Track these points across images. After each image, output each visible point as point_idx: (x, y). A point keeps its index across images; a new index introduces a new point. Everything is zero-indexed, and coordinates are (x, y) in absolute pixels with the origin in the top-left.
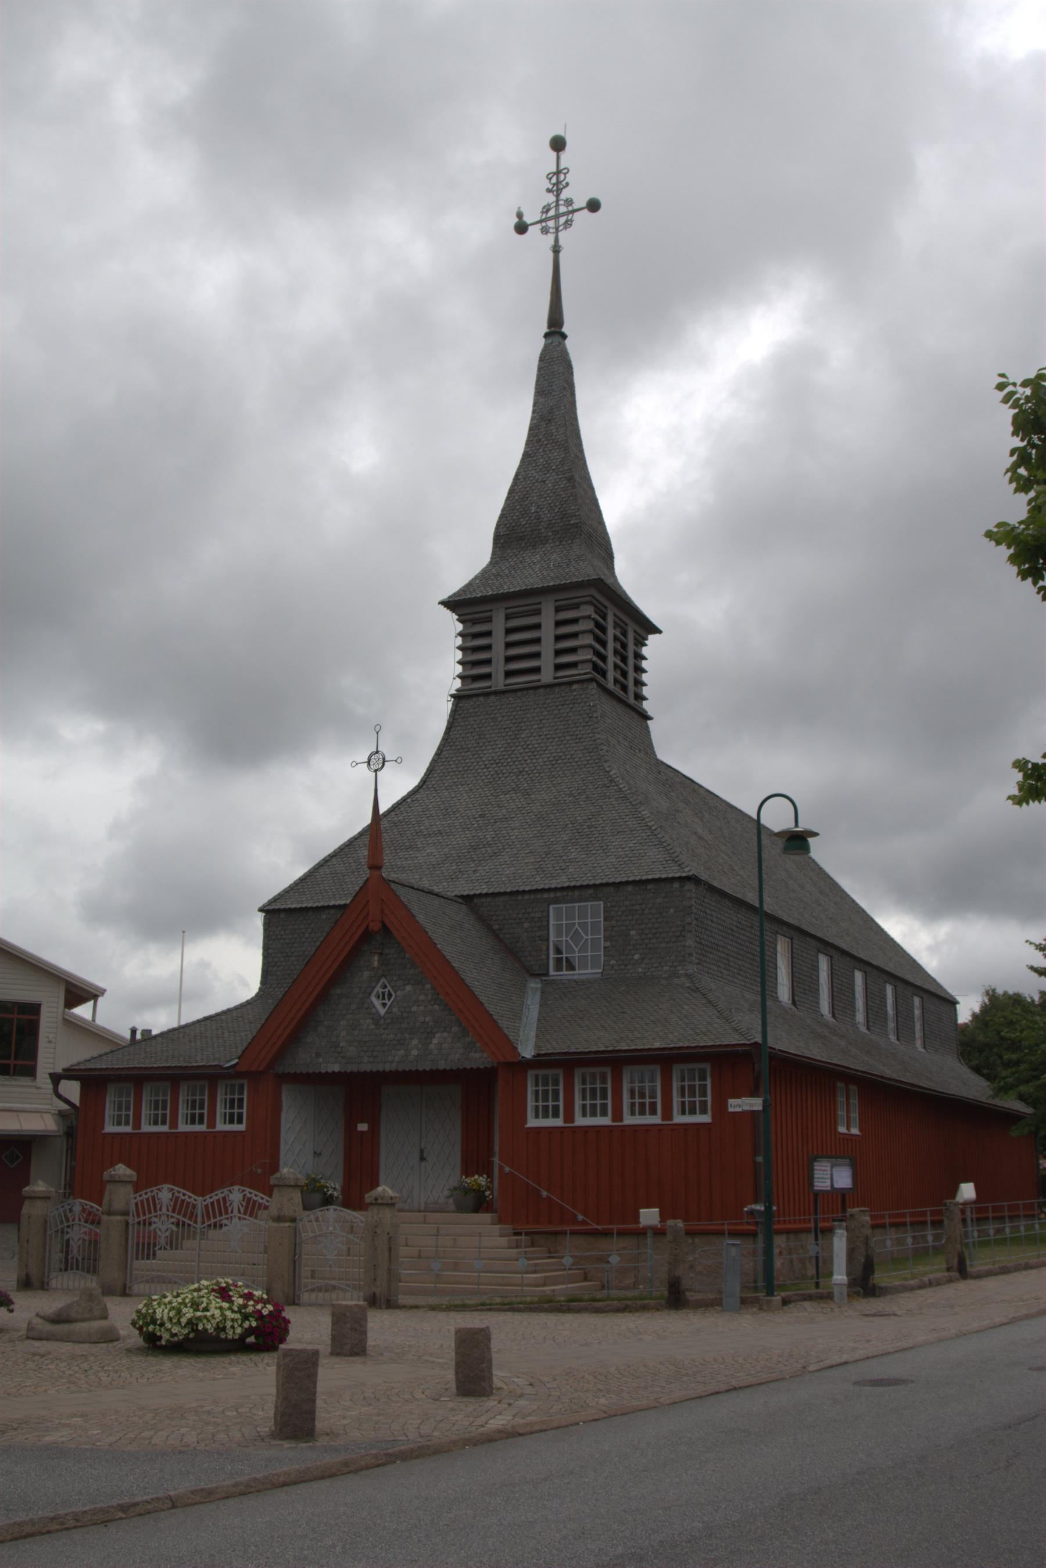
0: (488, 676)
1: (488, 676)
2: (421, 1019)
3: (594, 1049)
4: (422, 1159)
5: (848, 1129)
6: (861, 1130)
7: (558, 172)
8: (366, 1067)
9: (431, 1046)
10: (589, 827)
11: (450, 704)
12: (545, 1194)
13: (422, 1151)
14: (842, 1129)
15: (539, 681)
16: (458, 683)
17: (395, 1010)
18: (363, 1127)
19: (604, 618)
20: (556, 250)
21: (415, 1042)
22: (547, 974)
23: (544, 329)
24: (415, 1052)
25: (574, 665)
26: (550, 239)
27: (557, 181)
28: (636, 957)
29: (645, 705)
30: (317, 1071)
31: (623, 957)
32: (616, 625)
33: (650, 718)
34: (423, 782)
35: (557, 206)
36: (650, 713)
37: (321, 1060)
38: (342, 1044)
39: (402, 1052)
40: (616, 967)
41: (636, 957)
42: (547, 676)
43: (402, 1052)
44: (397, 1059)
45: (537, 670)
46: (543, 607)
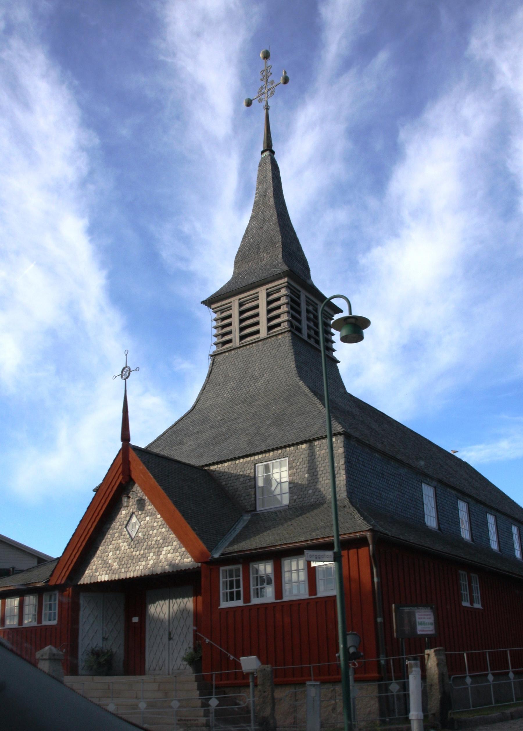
0: (230, 341)
1: (230, 341)
2: (155, 539)
3: (259, 546)
4: (170, 639)
5: (472, 603)
6: (482, 606)
8: (123, 576)
9: (161, 557)
10: (282, 415)
11: (210, 361)
12: (232, 657)
13: (170, 634)
14: (466, 604)
15: (259, 338)
16: (214, 348)
17: (140, 534)
18: (135, 620)
19: (299, 297)
21: (151, 554)
22: (255, 510)
24: (151, 562)
25: (279, 325)
28: (310, 492)
29: (335, 354)
30: (96, 581)
31: (302, 493)
32: (308, 303)
33: (339, 362)
34: (194, 407)
36: (338, 359)
37: (98, 574)
38: (110, 561)
39: (144, 563)
40: (297, 500)
41: (310, 492)
43: (144, 563)
44: (141, 567)
45: (257, 332)
46: (260, 295)
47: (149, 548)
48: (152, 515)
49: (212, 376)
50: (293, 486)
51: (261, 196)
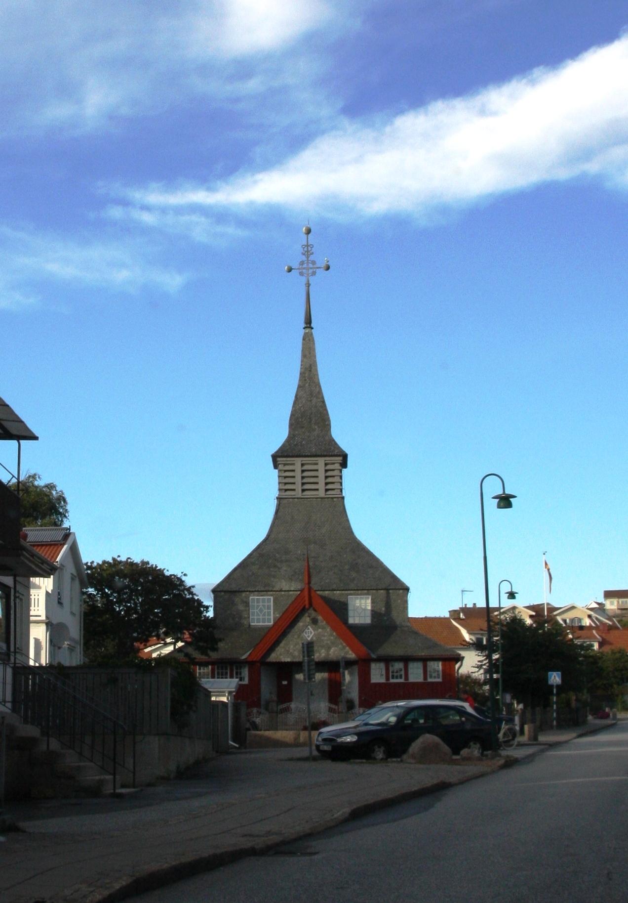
7: (308, 246)
18: (285, 683)
20: (308, 285)
23: (304, 325)
26: (303, 280)
27: (307, 250)
34: (268, 536)
35: (308, 263)
42: (321, 493)
47: (323, 647)
48: (323, 628)
49: (279, 514)
50: (375, 614)
51: (306, 369)
